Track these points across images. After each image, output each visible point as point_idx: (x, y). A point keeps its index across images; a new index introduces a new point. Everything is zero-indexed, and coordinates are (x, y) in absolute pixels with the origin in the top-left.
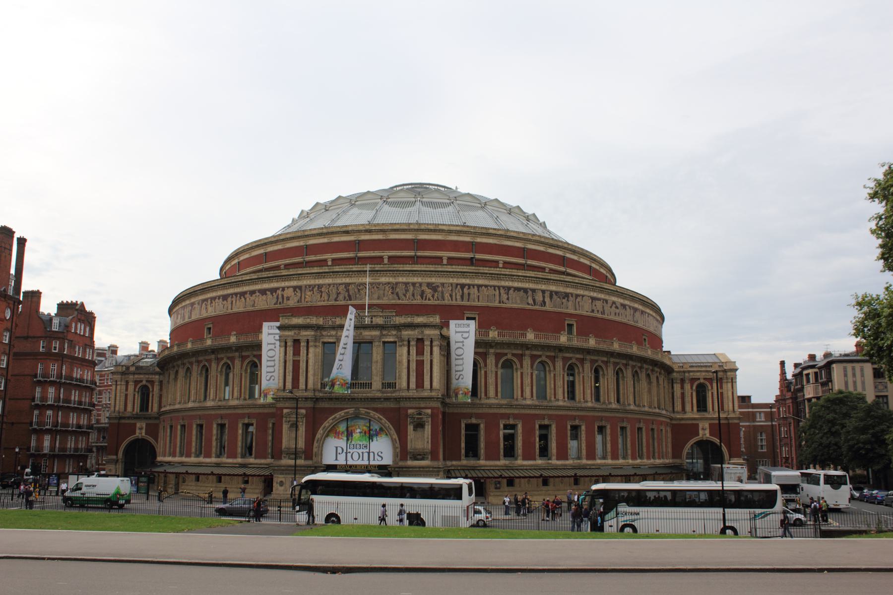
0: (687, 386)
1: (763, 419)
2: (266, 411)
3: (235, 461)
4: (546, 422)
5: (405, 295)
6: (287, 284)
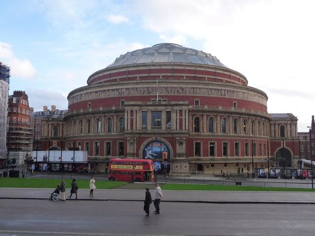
0: (277, 127)
1: (302, 139)
6: (123, 87)
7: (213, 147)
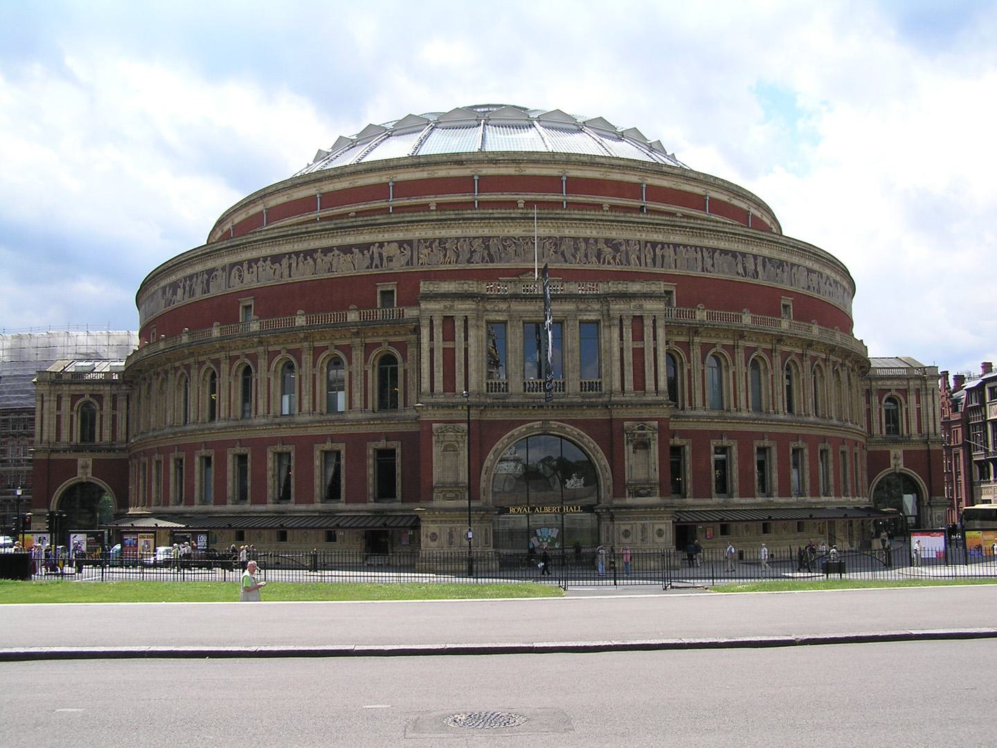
2: (363, 430)
3: (311, 507)
4: (766, 443)
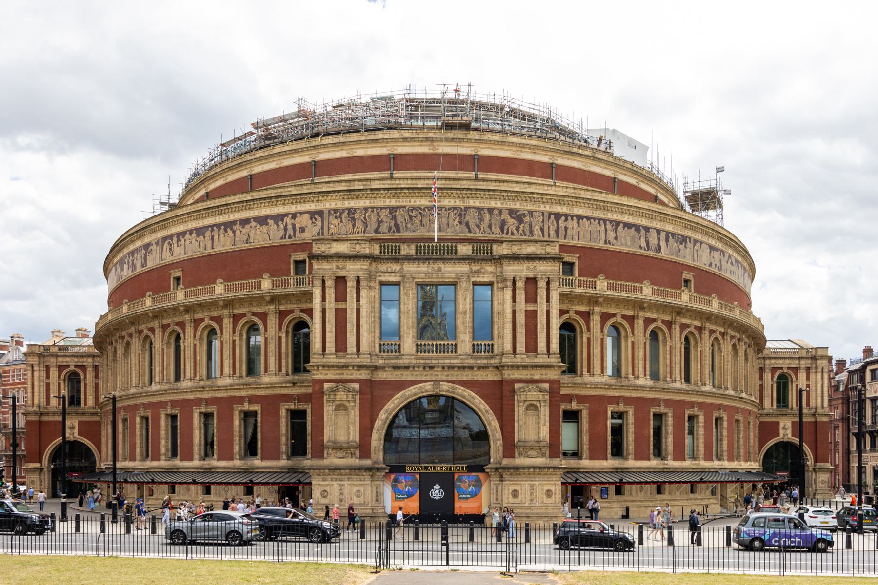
5: (478, 227)
6: (300, 207)
7: (621, 426)
